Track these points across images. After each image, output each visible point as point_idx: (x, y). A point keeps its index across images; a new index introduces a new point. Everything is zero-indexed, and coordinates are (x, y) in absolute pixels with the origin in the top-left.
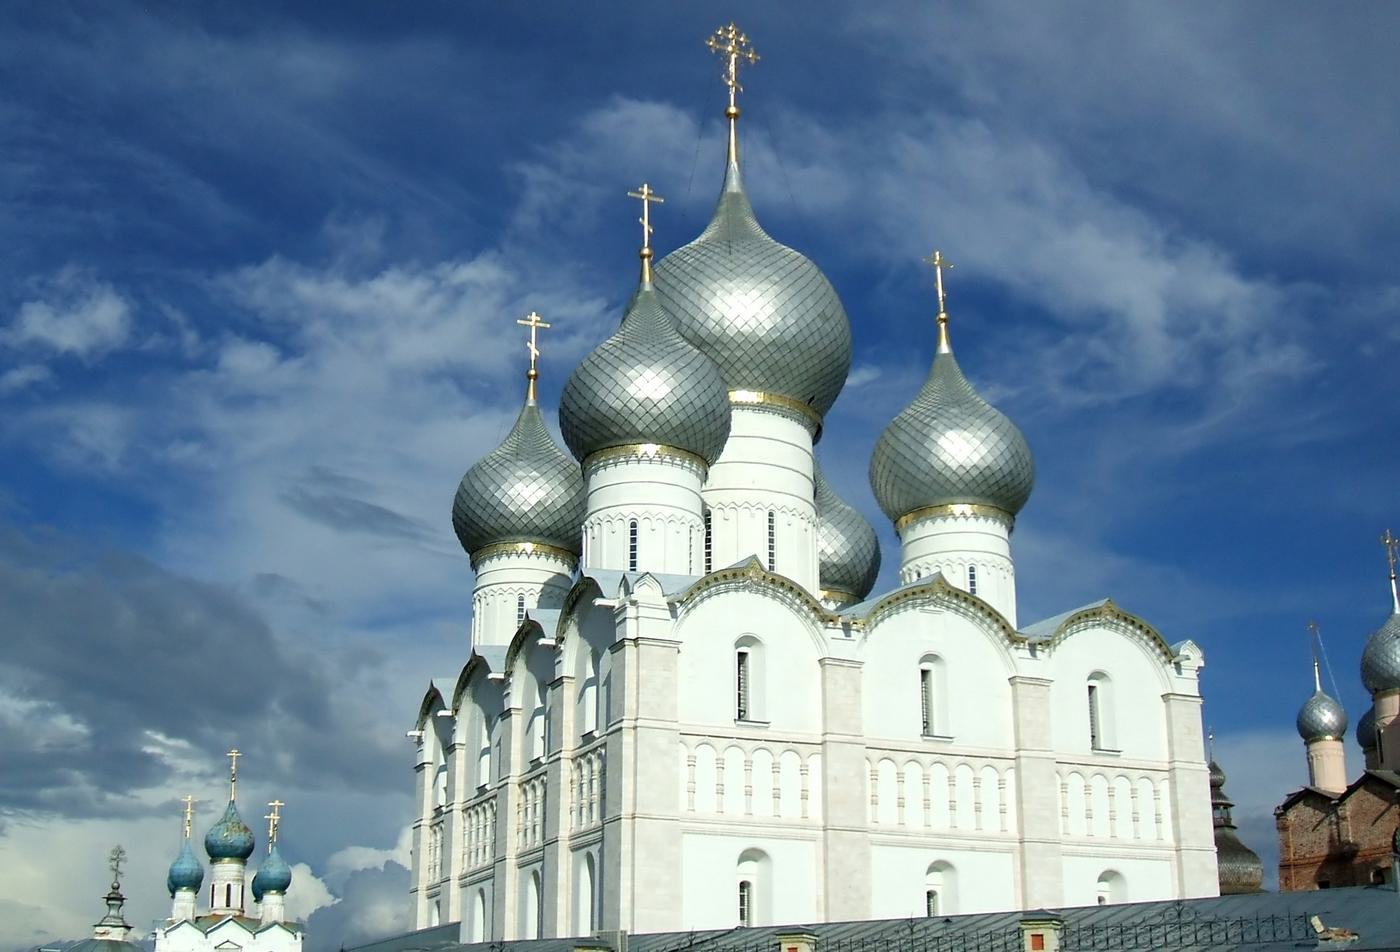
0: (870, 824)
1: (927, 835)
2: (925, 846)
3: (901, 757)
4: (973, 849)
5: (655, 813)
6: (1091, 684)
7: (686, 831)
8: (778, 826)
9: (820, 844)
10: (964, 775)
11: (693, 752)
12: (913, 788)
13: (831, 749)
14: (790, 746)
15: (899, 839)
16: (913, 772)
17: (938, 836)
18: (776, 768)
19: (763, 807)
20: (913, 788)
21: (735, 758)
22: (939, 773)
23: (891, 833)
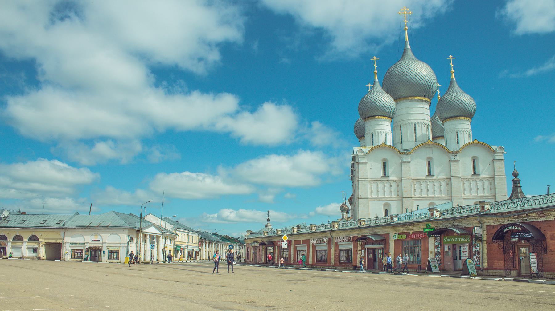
0: (413, 196)
4: (440, 200)
5: (363, 197)
9: (401, 201)
15: (422, 199)
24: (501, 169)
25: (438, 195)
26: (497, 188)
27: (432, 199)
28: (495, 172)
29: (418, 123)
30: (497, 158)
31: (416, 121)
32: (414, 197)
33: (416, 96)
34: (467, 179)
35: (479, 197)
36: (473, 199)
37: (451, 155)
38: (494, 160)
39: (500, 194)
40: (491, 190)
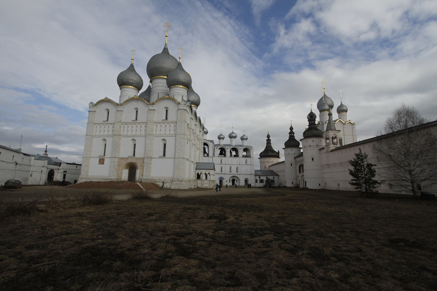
1: (131, 135)
2: (131, 137)
3: (128, 124)
4: (139, 137)
6: (167, 109)
7: (94, 137)
8: (108, 135)
10: (139, 126)
11: (97, 126)
12: (130, 129)
13: (116, 124)
14: (111, 124)
15: (127, 136)
16: (130, 126)
17: (133, 135)
18: (109, 127)
19: (106, 133)
20: (130, 129)
21: (103, 126)
22: (135, 126)
23: (125, 135)
24: (182, 116)
25: (138, 133)
26: (178, 129)
27: (134, 136)
28: (178, 118)
29: (161, 92)
30: (180, 108)
31: (159, 91)
32: (122, 135)
33: (161, 75)
34: (159, 123)
35: (165, 136)
36: (161, 137)
37: (149, 106)
38: (178, 109)
39: (179, 133)
40: (174, 130)
